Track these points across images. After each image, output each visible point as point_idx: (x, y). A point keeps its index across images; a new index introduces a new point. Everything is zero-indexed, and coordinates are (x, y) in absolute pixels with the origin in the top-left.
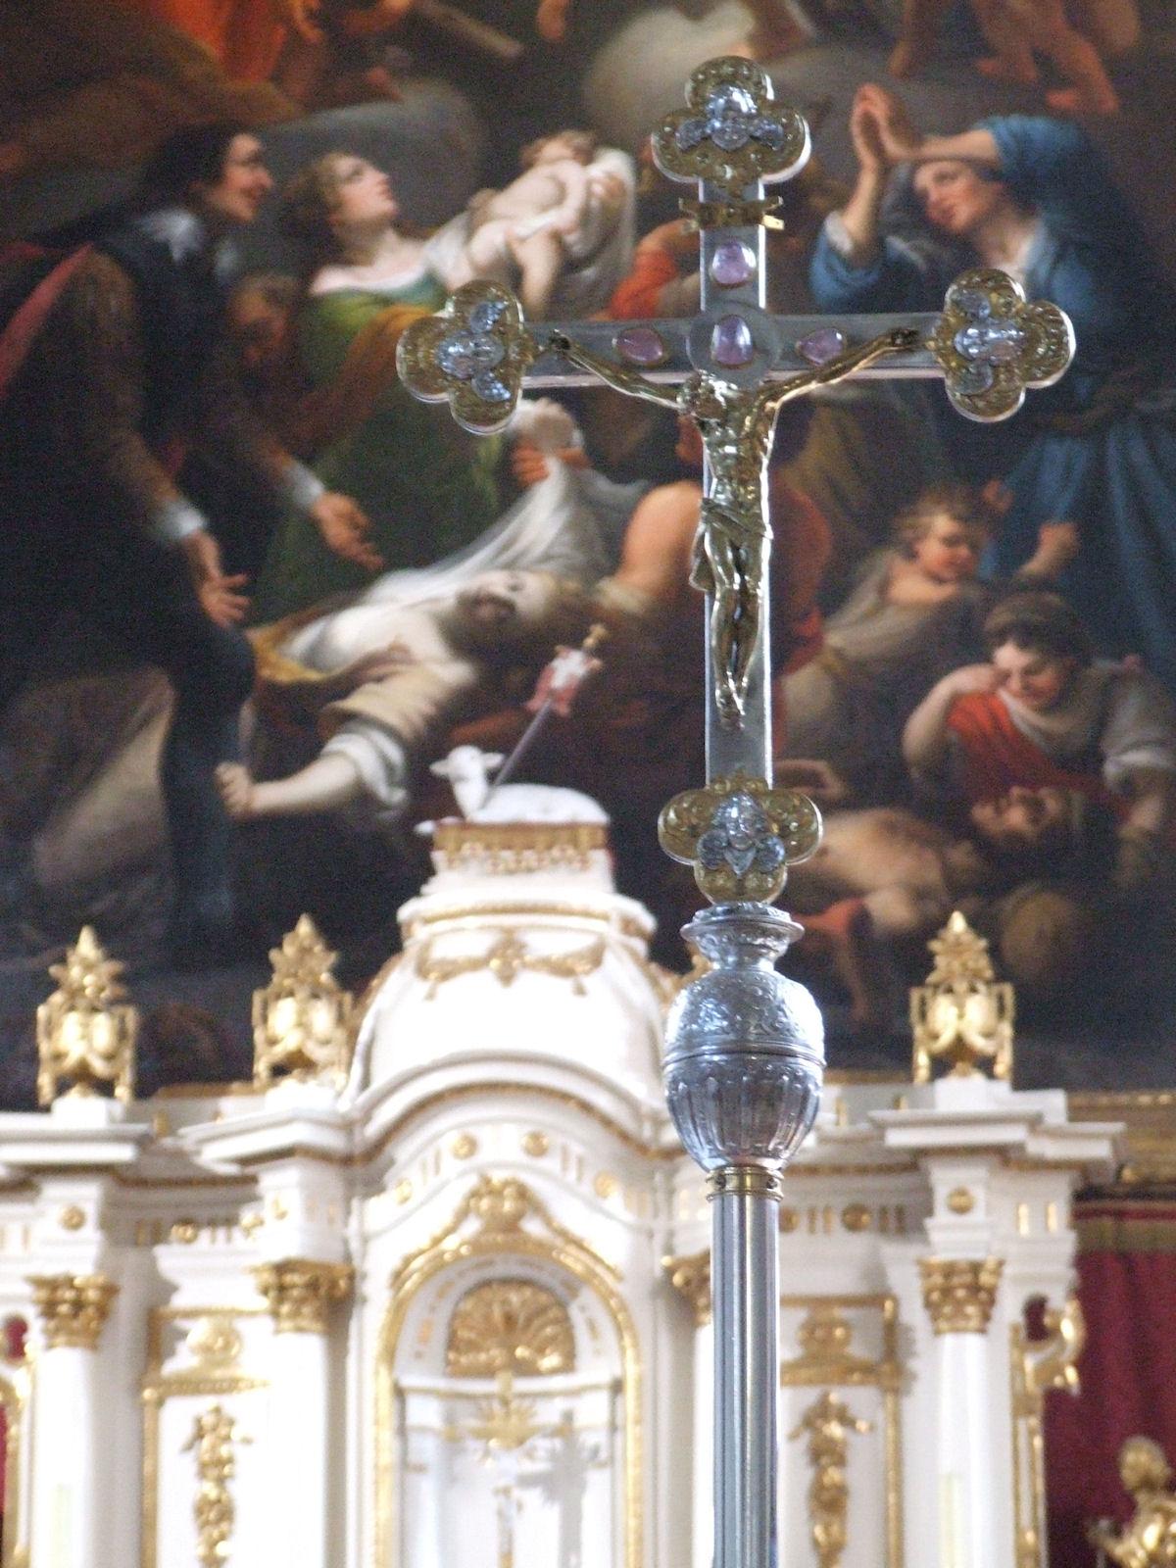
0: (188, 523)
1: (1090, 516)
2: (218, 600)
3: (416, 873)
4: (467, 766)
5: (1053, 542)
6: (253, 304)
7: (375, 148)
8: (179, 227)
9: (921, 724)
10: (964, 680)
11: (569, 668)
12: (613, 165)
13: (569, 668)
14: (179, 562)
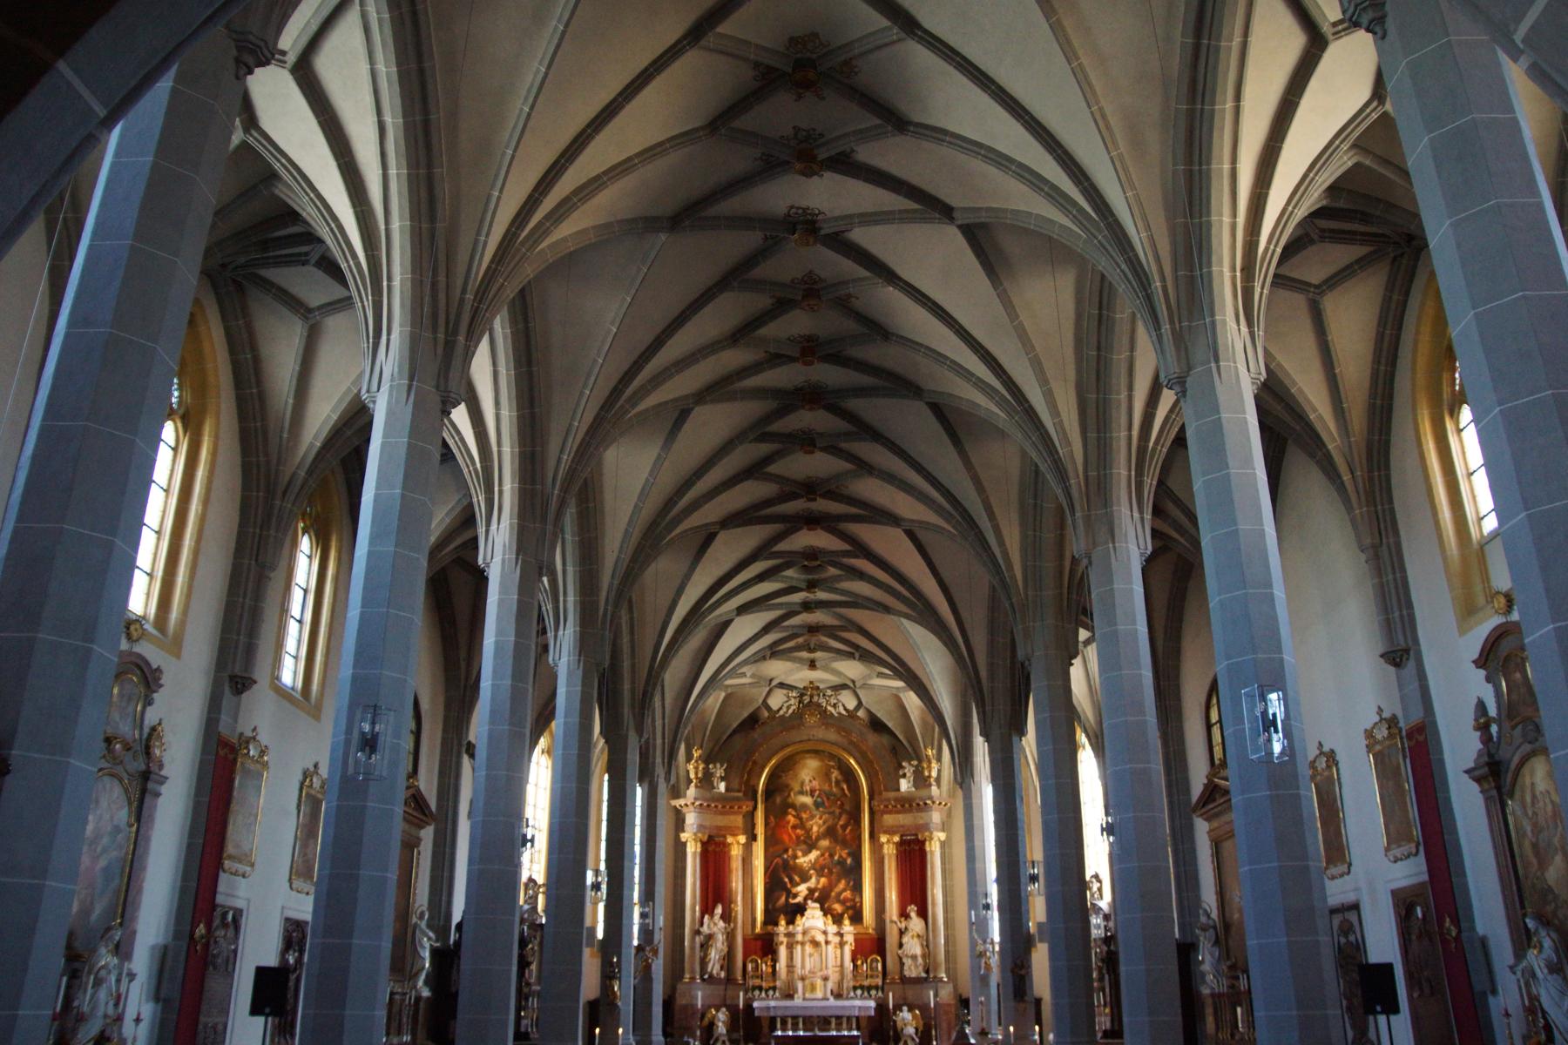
0: (786, 880)
1: (854, 880)
2: (789, 886)
3: (805, 910)
4: (809, 902)
5: (852, 883)
6: (791, 862)
7: (801, 850)
8: (785, 856)
9: (842, 897)
10: (844, 894)
11: (817, 894)
12: (818, 852)
13: (817, 894)
14: (785, 883)
